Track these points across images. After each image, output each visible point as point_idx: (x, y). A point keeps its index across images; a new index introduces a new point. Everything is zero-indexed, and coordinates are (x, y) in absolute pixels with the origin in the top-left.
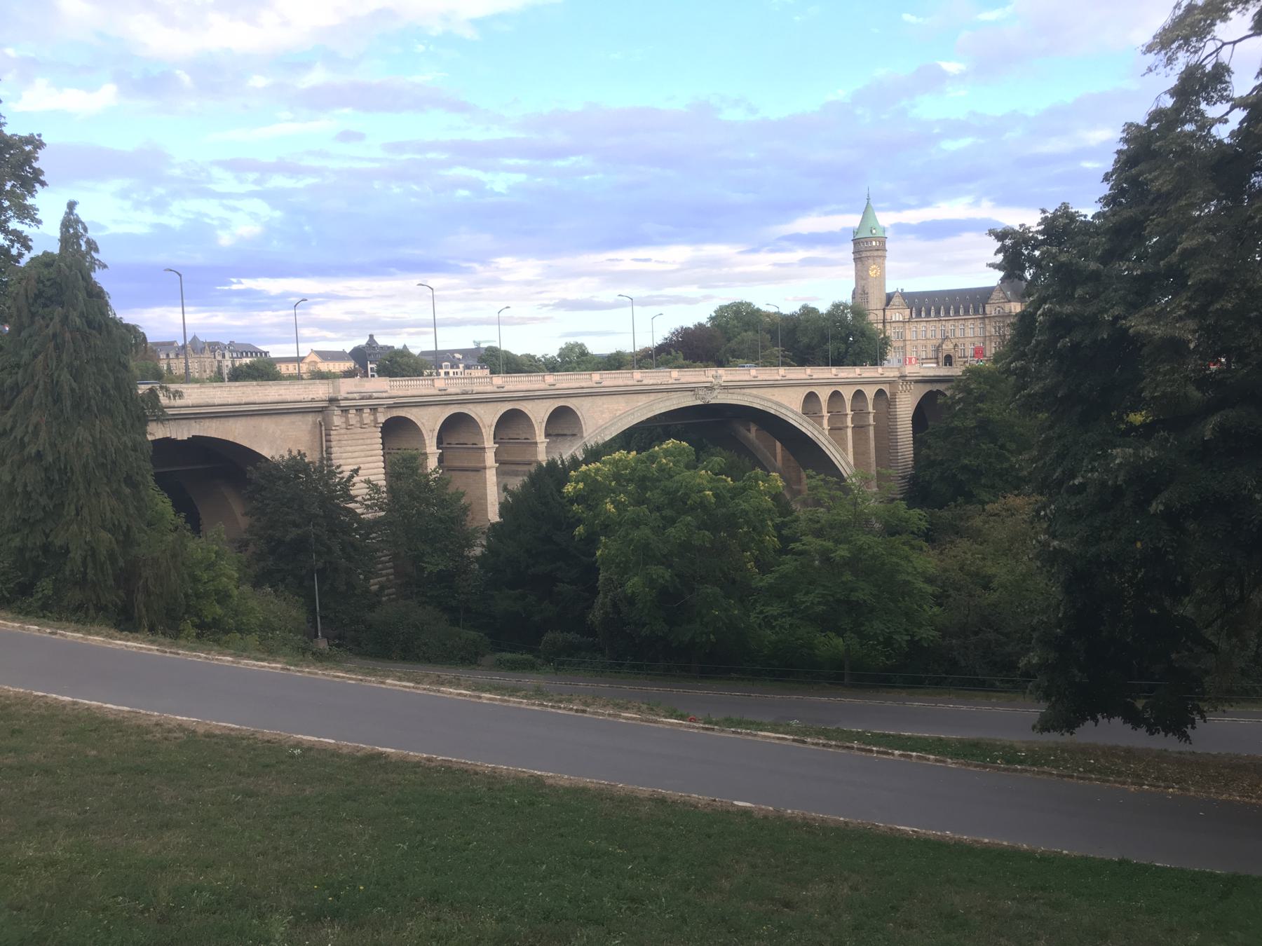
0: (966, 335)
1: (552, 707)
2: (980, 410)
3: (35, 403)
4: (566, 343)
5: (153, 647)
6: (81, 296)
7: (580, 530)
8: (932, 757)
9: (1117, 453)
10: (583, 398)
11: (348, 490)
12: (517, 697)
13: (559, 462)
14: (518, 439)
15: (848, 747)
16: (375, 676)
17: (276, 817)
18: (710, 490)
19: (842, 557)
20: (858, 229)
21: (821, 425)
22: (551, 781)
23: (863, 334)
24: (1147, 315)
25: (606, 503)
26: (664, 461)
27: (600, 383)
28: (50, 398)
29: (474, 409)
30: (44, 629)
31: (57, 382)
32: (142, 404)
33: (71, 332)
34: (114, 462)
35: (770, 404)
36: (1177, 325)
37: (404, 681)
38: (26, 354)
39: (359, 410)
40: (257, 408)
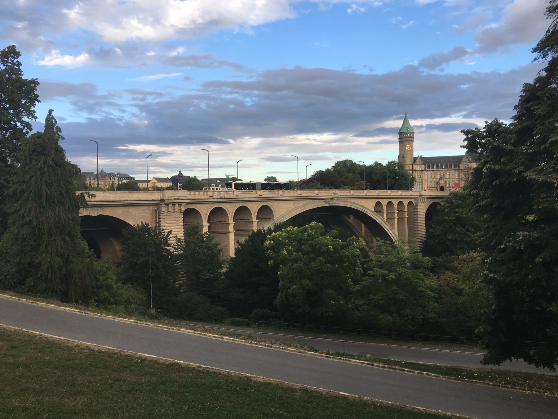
0: (450, 177)
1: (256, 344)
2: (457, 212)
3: (30, 198)
4: (267, 177)
5: (77, 310)
6: (53, 151)
7: (271, 262)
8: (433, 374)
9: (521, 234)
10: (274, 202)
11: (167, 241)
12: (240, 339)
13: (262, 231)
14: (244, 220)
15: (393, 368)
16: (176, 327)
17: (128, 391)
18: (331, 245)
19: (392, 278)
20: (401, 128)
21: (383, 217)
22: (255, 379)
23: (403, 176)
24: (534, 171)
25: (283, 250)
26: (310, 231)
27: (282, 195)
28: (37, 197)
29: (225, 206)
30: (29, 300)
31: (40, 189)
32: (77, 200)
33: (47, 168)
34: (63, 226)
35: (359, 207)
36: (549, 176)
37: (189, 329)
38: (27, 177)
39: (174, 205)
40: (128, 203)
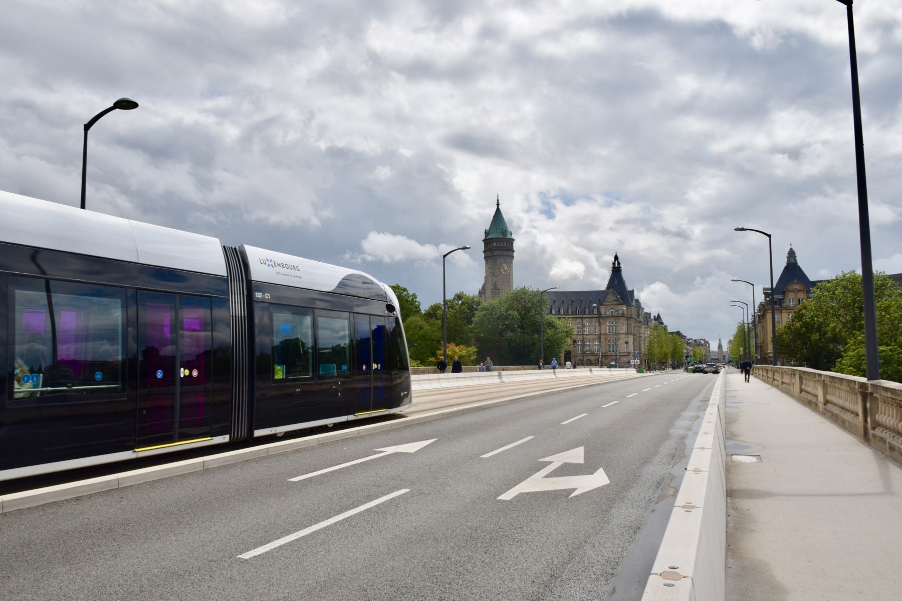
20: (489, 230)
